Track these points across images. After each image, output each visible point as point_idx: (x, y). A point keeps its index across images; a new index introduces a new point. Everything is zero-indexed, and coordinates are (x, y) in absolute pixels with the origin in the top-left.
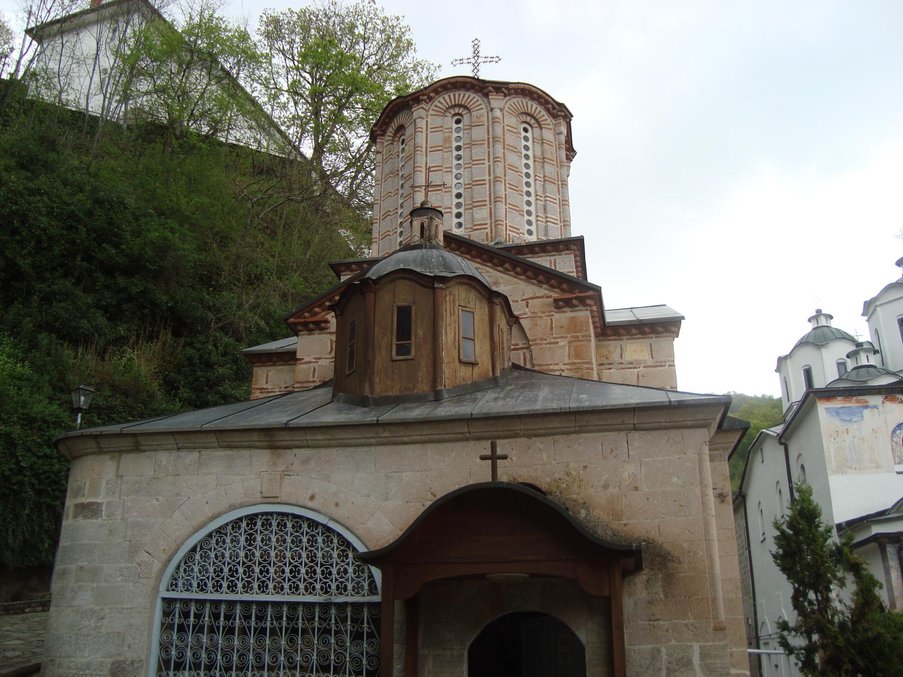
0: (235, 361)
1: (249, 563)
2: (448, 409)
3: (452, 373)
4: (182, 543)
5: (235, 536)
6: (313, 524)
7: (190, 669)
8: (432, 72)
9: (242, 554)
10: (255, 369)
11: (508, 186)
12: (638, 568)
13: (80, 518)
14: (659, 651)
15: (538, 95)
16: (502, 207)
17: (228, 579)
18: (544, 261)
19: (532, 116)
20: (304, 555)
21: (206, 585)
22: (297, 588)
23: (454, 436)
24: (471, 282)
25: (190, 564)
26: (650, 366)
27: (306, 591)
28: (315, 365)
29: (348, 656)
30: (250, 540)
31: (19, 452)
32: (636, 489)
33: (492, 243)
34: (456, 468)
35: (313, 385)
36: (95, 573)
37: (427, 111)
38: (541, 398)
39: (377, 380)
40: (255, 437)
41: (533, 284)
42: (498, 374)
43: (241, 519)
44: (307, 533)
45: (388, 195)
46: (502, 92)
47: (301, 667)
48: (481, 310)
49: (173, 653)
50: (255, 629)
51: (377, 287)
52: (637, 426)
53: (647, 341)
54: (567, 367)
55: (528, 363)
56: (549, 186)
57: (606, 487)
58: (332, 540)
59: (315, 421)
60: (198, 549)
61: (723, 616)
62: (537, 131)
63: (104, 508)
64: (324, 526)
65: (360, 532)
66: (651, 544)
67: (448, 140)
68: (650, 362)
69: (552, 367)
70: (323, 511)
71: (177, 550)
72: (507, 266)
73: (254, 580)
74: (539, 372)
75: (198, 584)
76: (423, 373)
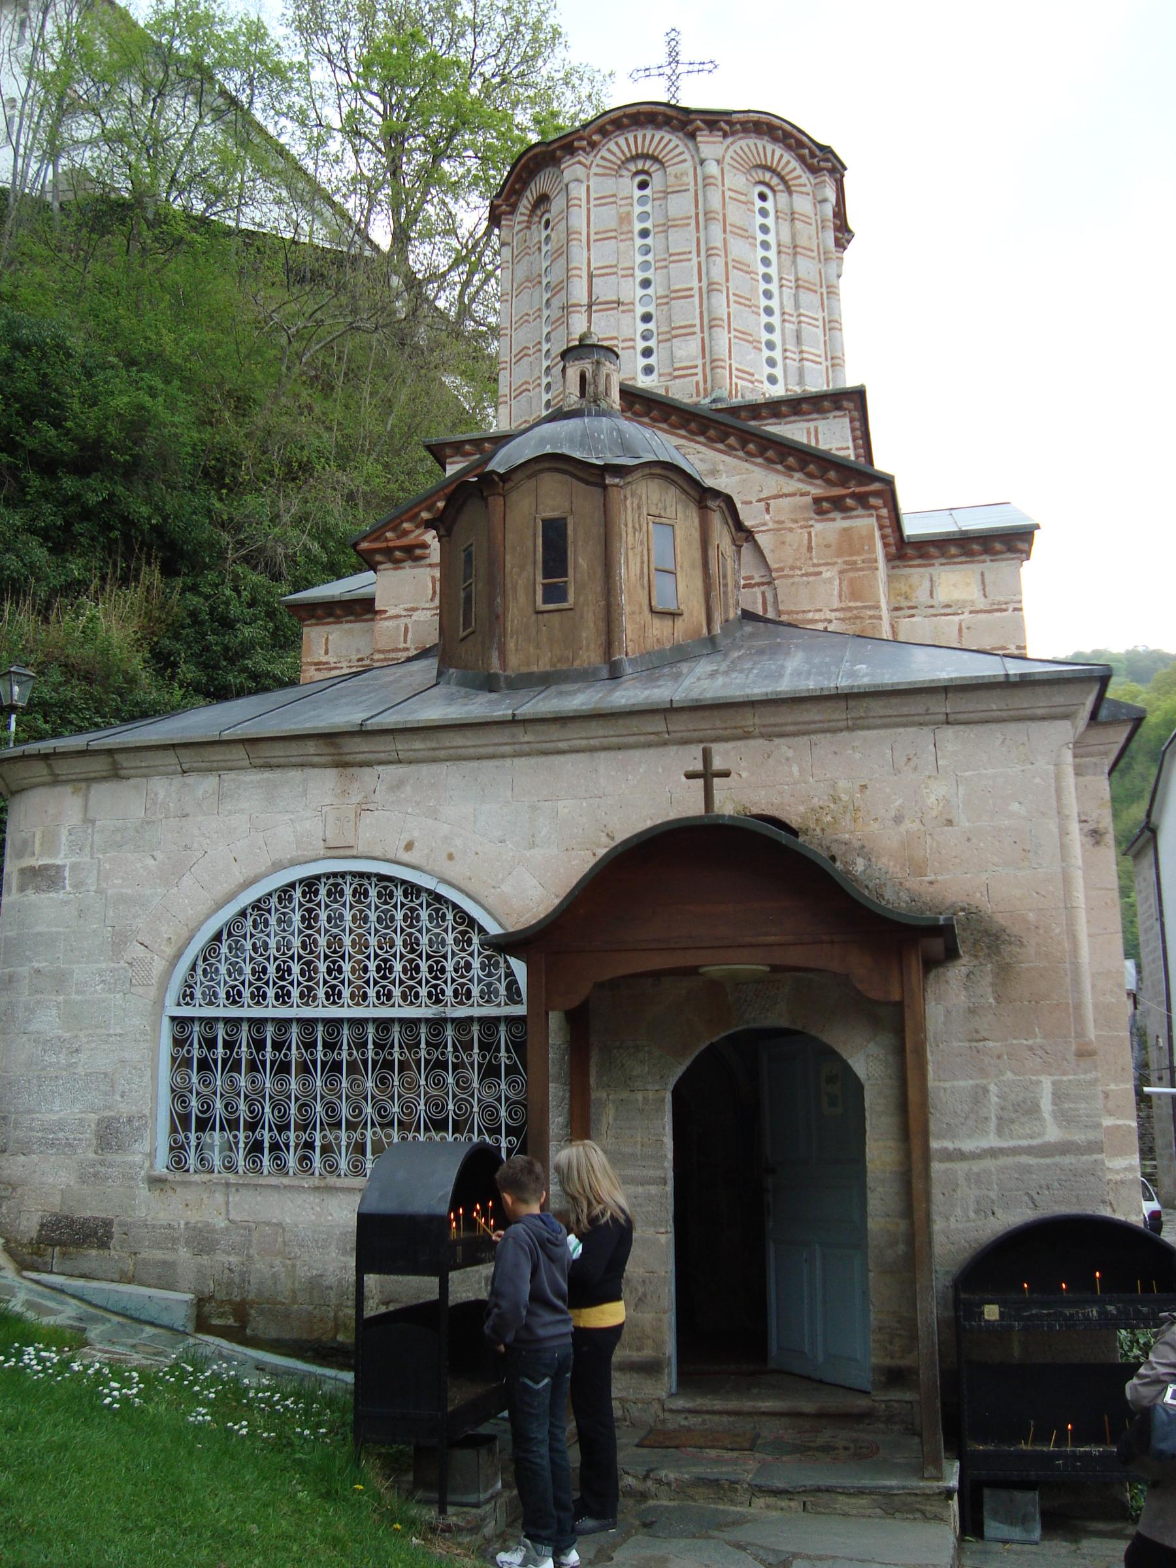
0: (271, 614)
1: (310, 957)
2: (631, 693)
3: (638, 631)
4: (198, 928)
5: (284, 914)
6: (412, 890)
7: (222, 1129)
8: (598, 86)
9: (297, 942)
10: (305, 630)
11: (732, 298)
12: (952, 954)
13: (30, 892)
14: (986, 1090)
15: (784, 131)
16: (722, 338)
17: (275, 983)
18: (795, 431)
19: (773, 171)
20: (399, 941)
21: (240, 994)
22: (389, 996)
23: (642, 739)
24: (669, 472)
25: (213, 961)
26: (981, 611)
27: (405, 1000)
28: (407, 620)
29: (475, 1104)
30: (309, 918)
32: (950, 822)
33: (708, 400)
34: (647, 792)
35: (405, 655)
36: (60, 980)
37: (588, 168)
38: (788, 671)
39: (511, 645)
40: (311, 747)
41: (777, 471)
42: (717, 630)
43: (292, 885)
44: (403, 905)
45: (524, 319)
46: (721, 129)
47: (400, 1123)
48: (686, 521)
49: (194, 1103)
50: (324, 1064)
51: (507, 486)
52: (951, 718)
53: (976, 568)
54: (838, 614)
55: (770, 609)
56: (804, 296)
57: (898, 819)
58: (444, 915)
59: (410, 718)
60: (225, 936)
61: (1092, 1033)
62: (783, 197)
63: (67, 874)
64: (430, 892)
65: (489, 901)
66: (973, 915)
67: (625, 219)
68: (981, 604)
69: (810, 616)
70: (428, 868)
71: (190, 939)
72: (732, 440)
73: (317, 984)
74: (790, 625)
75: (228, 993)
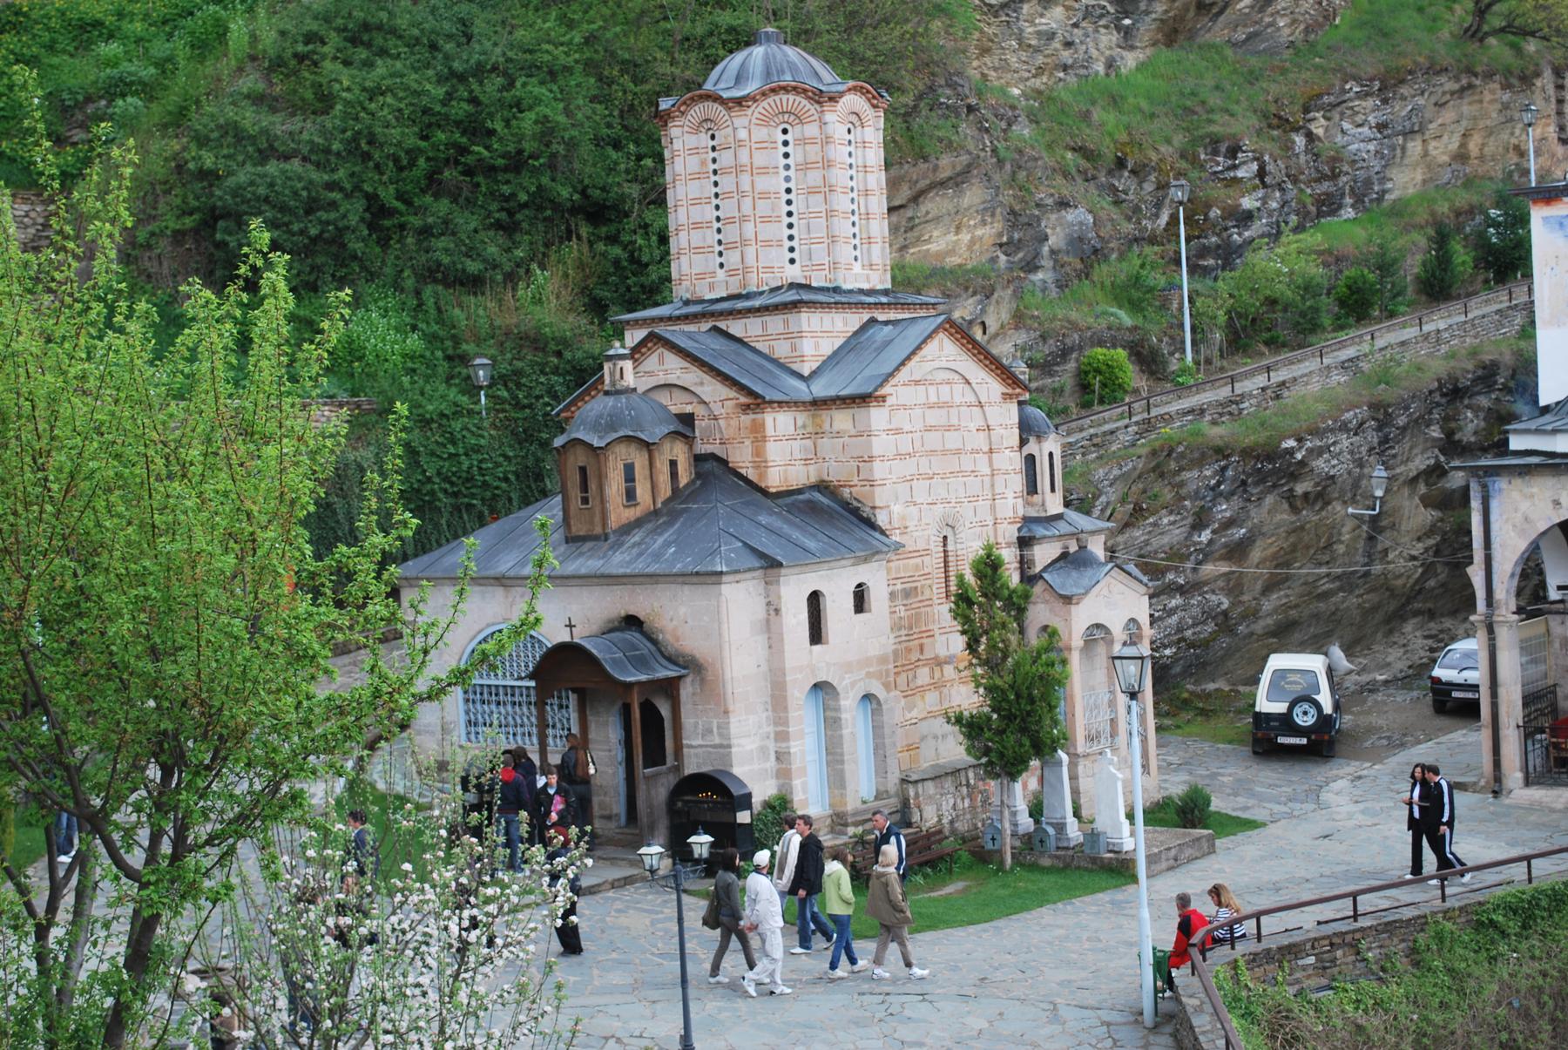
31: (423, 460)
53: (851, 411)
56: (812, 198)
68: (853, 432)
76: (597, 519)
